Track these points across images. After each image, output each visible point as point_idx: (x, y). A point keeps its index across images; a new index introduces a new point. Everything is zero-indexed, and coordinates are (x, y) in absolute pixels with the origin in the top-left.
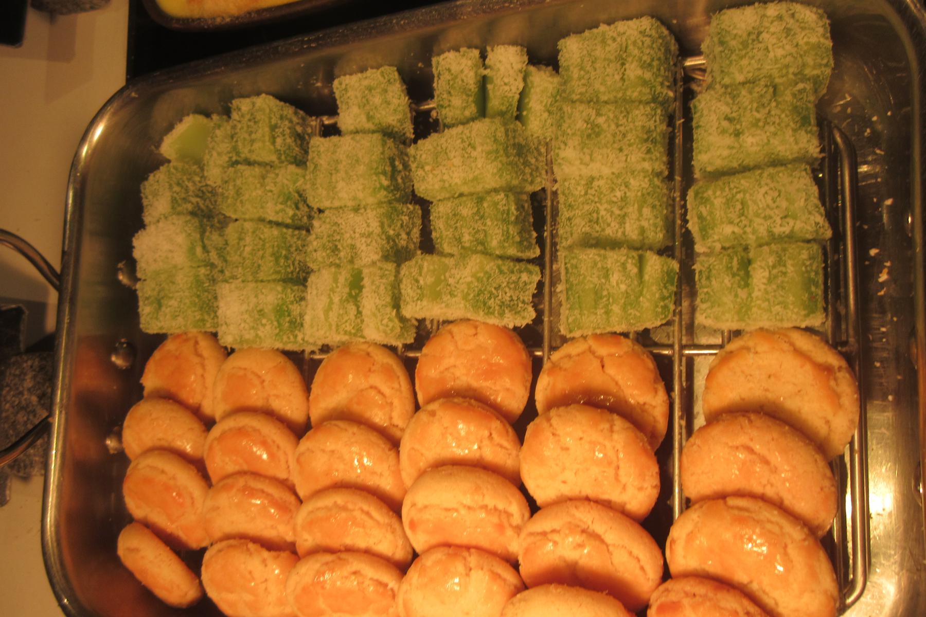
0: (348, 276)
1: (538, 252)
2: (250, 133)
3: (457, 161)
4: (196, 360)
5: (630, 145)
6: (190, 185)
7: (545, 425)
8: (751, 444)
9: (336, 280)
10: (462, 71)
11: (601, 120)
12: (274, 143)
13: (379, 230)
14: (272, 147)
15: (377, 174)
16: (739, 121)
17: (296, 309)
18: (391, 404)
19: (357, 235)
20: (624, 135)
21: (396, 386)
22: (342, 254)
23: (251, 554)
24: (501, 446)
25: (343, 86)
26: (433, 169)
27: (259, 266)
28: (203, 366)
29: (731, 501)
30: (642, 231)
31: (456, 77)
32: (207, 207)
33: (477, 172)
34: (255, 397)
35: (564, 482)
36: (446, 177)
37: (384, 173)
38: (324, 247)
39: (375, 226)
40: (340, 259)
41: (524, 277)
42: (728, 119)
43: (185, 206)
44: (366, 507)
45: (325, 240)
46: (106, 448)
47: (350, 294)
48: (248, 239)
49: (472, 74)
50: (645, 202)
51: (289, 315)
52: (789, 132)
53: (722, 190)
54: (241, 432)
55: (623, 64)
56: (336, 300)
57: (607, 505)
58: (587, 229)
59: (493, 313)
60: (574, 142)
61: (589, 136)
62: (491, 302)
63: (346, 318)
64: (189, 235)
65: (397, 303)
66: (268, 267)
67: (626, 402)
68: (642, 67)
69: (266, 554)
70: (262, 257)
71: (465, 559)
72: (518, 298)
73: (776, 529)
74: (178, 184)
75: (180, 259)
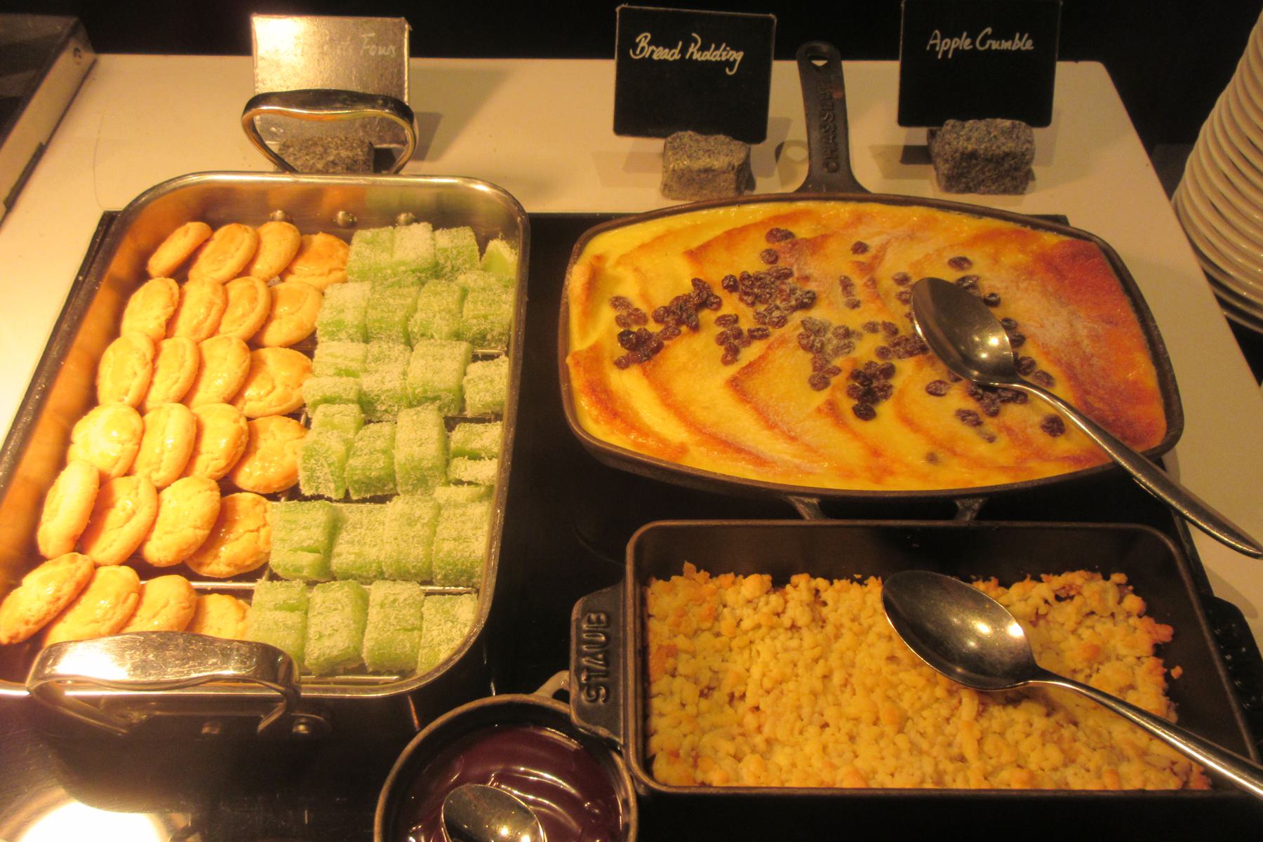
0: (353, 368)
1: (355, 498)
2: (482, 301)
3: (413, 435)
4: (326, 269)
5: (398, 545)
6: (460, 261)
7: (207, 487)
8: (168, 608)
9: (352, 360)
10: (481, 440)
11: (419, 526)
12: (474, 317)
13: (385, 388)
14: (470, 316)
15: (423, 385)
16: (390, 607)
17: (343, 335)
18: (261, 401)
19: (384, 374)
20: (405, 541)
21: (274, 404)
22: (373, 364)
23: (165, 308)
24: (207, 467)
25: (500, 364)
26: (412, 420)
27: (376, 309)
28: (322, 275)
29: (133, 597)
30: (339, 555)
31: (479, 436)
32: (446, 274)
33: (401, 448)
34: (282, 309)
35: (170, 501)
36: (404, 428)
37: (425, 391)
38: (382, 352)
39: (388, 386)
40: (370, 363)
41: (332, 486)
42: (395, 601)
43: (442, 258)
44: (181, 380)
45: (387, 353)
46: (275, 210)
47: (341, 370)
48: (398, 301)
49: (478, 446)
50: (447, 612)
51: (338, 331)
52: (375, 636)
53: (347, 597)
54: (254, 299)
55: (455, 540)
56: (339, 361)
57: (151, 527)
58: (351, 521)
59: (305, 462)
60: (407, 509)
61: (409, 518)
62: (313, 461)
63: (324, 367)
64: (414, 261)
65: (328, 401)
66: (373, 314)
67: (222, 545)
68: (448, 551)
69: (163, 319)
70: (382, 311)
71: (131, 441)
72: (320, 483)
73: (108, 616)
74: (459, 253)
75: (399, 255)
